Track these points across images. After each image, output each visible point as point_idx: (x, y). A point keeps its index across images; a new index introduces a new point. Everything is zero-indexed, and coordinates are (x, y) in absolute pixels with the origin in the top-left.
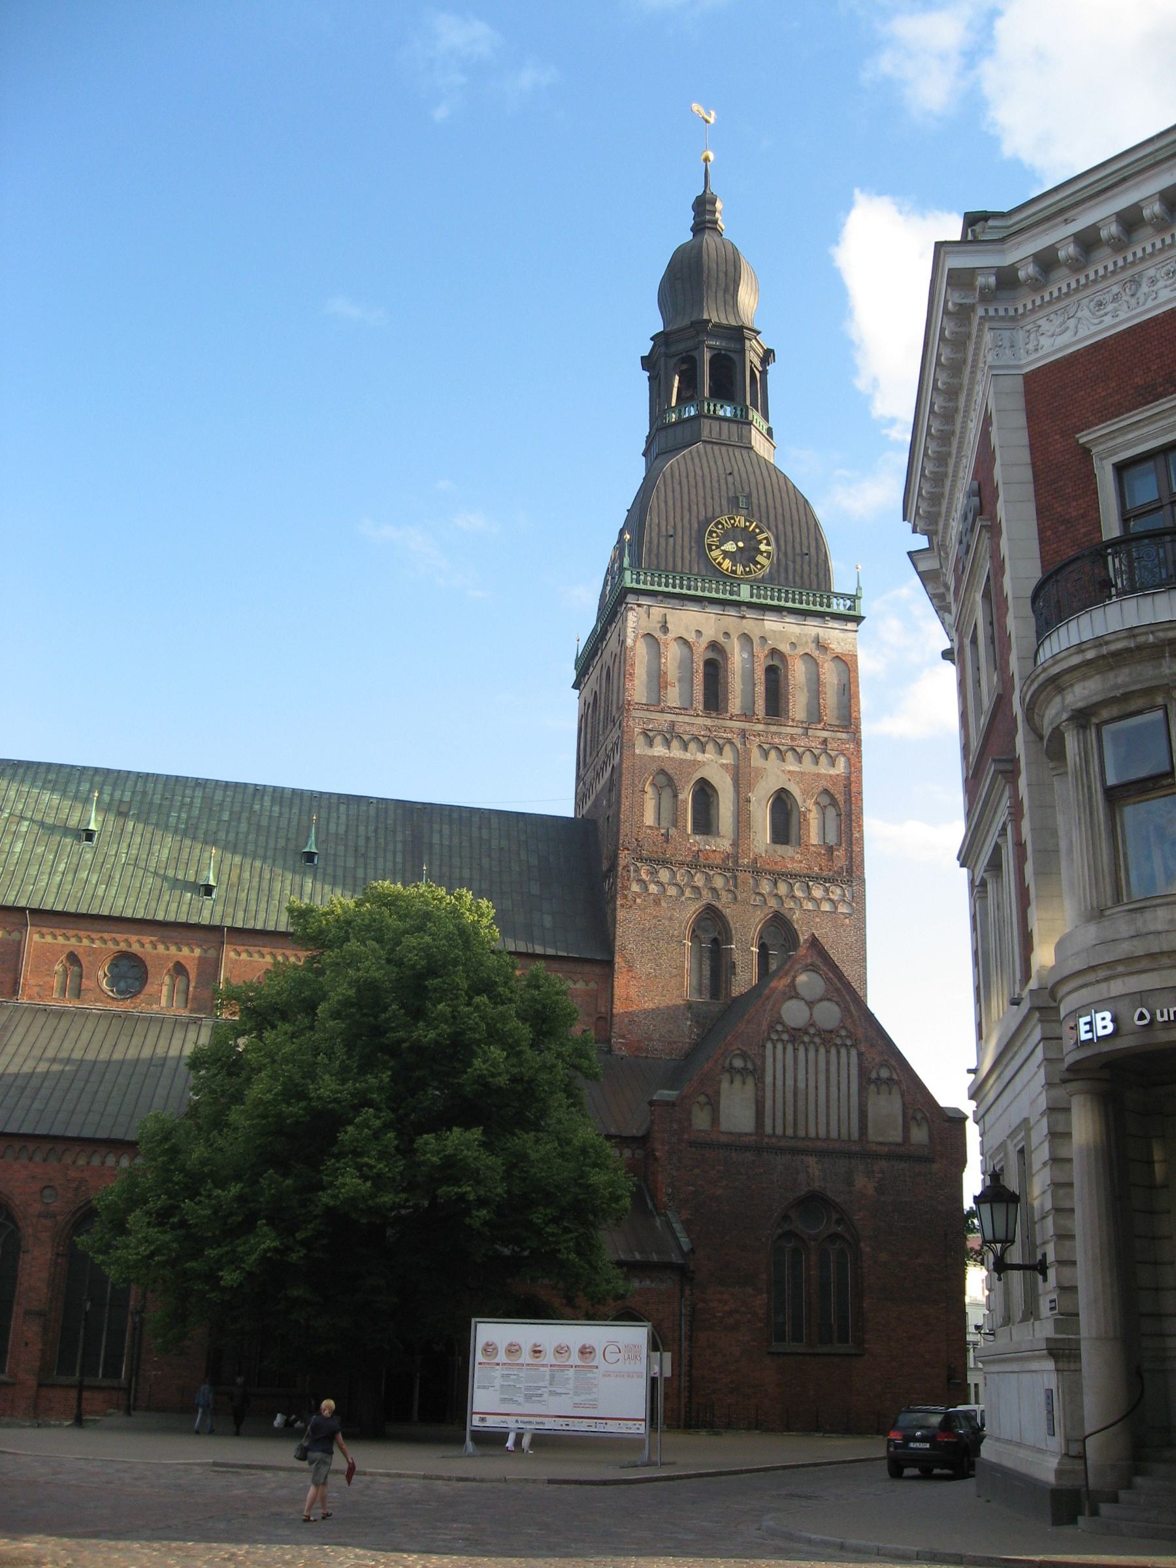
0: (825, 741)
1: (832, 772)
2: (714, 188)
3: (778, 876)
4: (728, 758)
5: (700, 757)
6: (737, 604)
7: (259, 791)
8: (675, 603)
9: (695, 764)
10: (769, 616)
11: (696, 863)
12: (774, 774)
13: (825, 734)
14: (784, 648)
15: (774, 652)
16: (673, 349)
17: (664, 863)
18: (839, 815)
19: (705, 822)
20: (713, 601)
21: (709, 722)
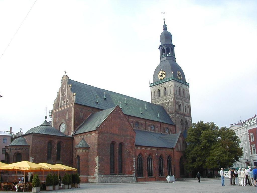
0: (188, 101)
1: (189, 104)
2: (166, 24)
3: (186, 116)
4: (182, 102)
5: (180, 101)
6: (181, 83)
7: (135, 99)
8: (176, 82)
9: (179, 102)
10: (183, 85)
11: (181, 114)
12: (185, 104)
13: (188, 100)
14: (184, 89)
15: (184, 89)
16: (167, 46)
17: (178, 114)
18: (189, 109)
19: (180, 110)
20: (178, 82)
21: (180, 97)
